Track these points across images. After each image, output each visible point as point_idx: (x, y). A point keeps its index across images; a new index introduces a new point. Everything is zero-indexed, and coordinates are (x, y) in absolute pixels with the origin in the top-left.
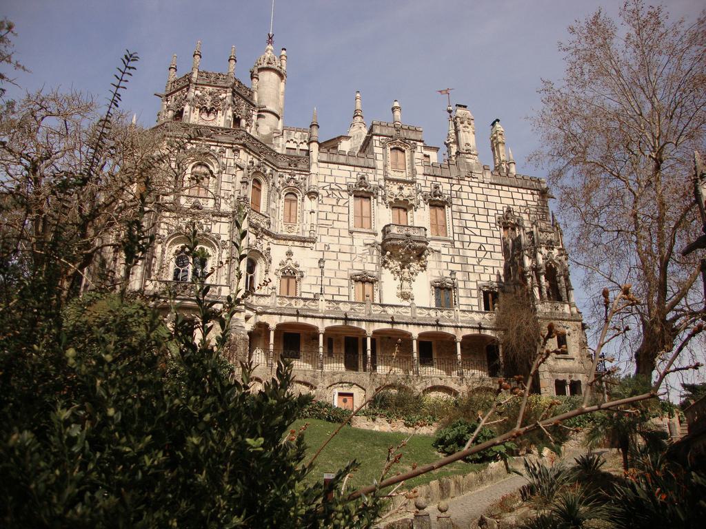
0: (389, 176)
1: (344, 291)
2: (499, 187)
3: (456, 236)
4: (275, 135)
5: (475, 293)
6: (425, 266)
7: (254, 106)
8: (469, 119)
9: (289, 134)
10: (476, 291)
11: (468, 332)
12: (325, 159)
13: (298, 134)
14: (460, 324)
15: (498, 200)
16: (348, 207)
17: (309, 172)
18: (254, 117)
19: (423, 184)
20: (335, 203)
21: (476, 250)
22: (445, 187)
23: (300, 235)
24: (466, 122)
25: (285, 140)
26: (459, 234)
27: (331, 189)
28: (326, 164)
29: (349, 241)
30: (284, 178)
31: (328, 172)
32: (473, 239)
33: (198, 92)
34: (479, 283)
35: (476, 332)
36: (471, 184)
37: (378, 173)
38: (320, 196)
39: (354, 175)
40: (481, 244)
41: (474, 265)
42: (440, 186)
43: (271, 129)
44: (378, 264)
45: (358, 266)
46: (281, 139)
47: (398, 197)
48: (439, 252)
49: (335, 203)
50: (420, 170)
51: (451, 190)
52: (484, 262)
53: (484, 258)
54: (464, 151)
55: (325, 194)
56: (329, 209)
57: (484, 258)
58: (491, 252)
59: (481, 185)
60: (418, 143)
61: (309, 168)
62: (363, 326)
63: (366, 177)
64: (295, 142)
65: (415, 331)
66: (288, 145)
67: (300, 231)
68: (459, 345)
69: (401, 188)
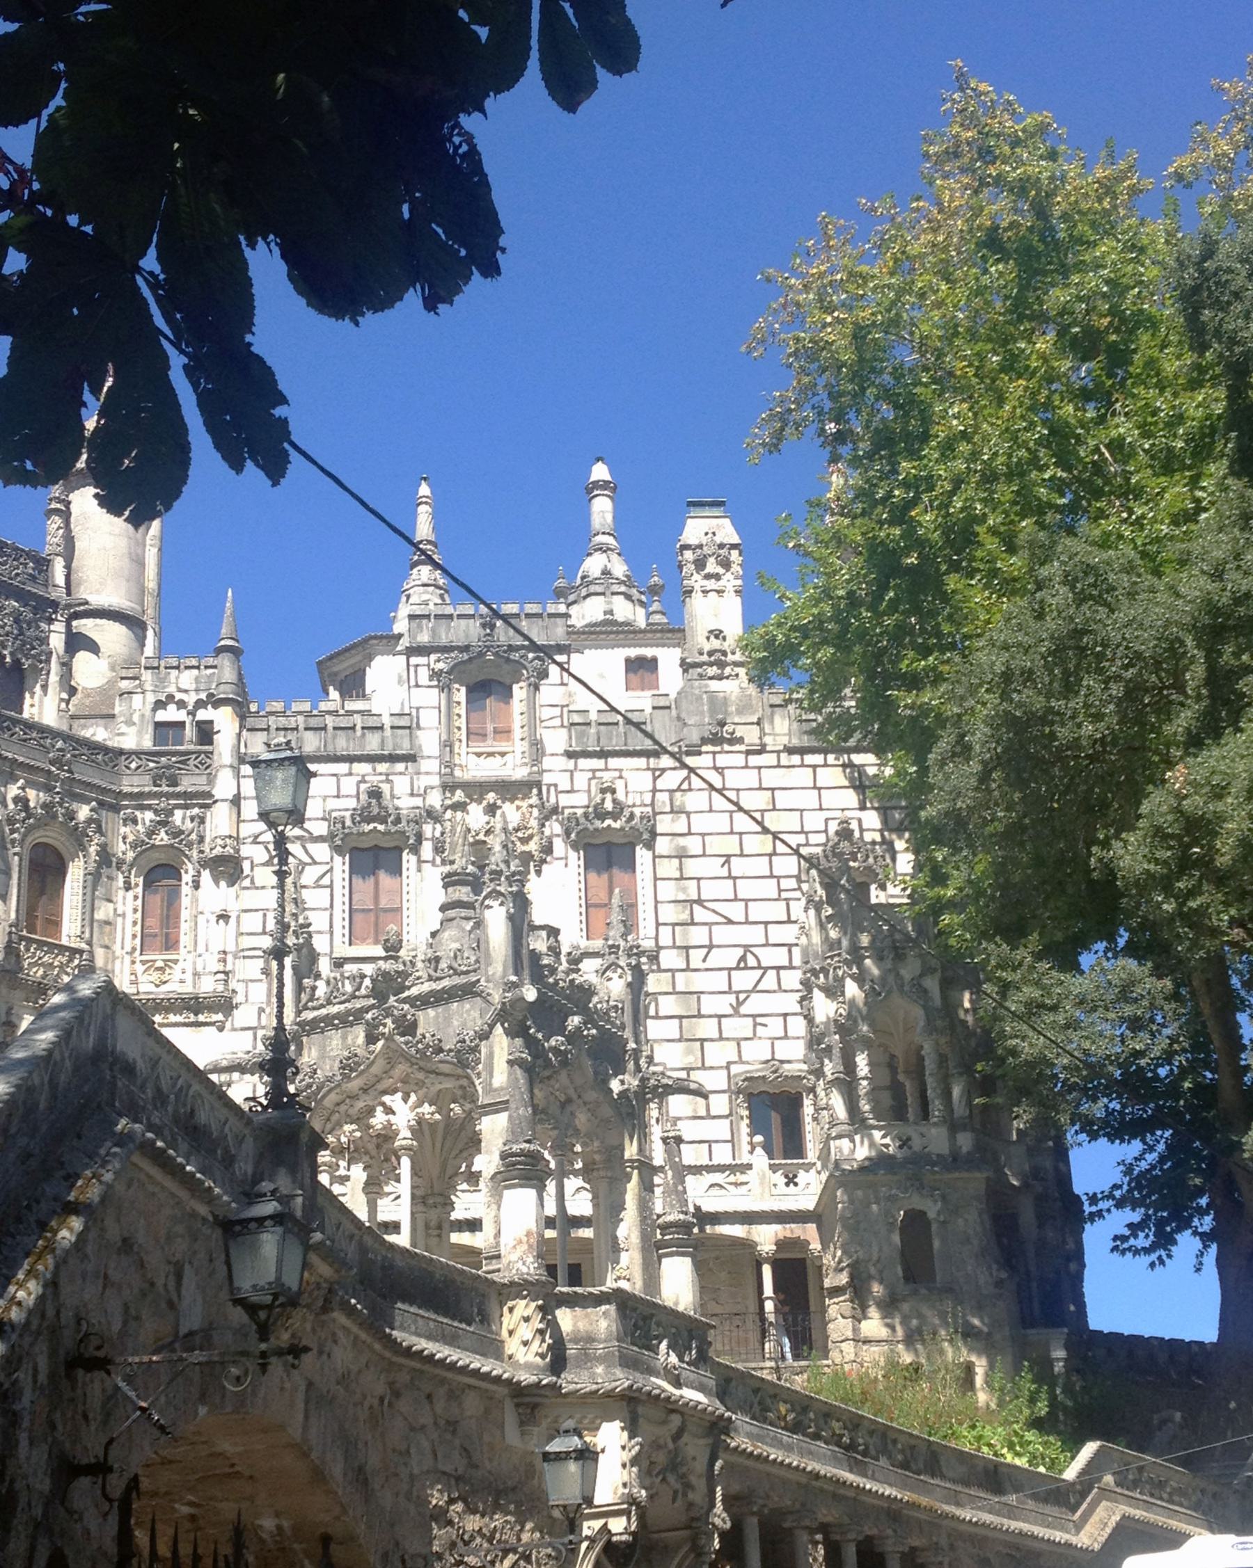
0: (458, 773)
2: (817, 759)
3: (665, 934)
4: (125, 685)
5: (720, 1104)
7: (54, 604)
8: (721, 546)
9: (161, 682)
10: (726, 1096)
15: (810, 799)
16: (331, 886)
17: (209, 795)
19: (564, 785)
21: (730, 969)
22: (634, 781)
23: (190, 990)
24: (712, 560)
25: (151, 698)
26: (674, 925)
30: (140, 827)
32: (722, 934)
34: (735, 1069)
36: (722, 760)
37: (423, 770)
38: (246, 866)
39: (349, 786)
40: (747, 948)
41: (720, 1017)
42: (619, 786)
43: (113, 669)
46: (137, 700)
47: (481, 837)
50: (556, 740)
51: (654, 791)
52: (754, 1004)
53: (754, 990)
54: (705, 658)
57: (754, 990)
58: (778, 968)
59: (754, 760)
61: (211, 780)
63: (385, 788)
64: (181, 704)
66: (162, 716)
67: (188, 977)
69: (491, 810)
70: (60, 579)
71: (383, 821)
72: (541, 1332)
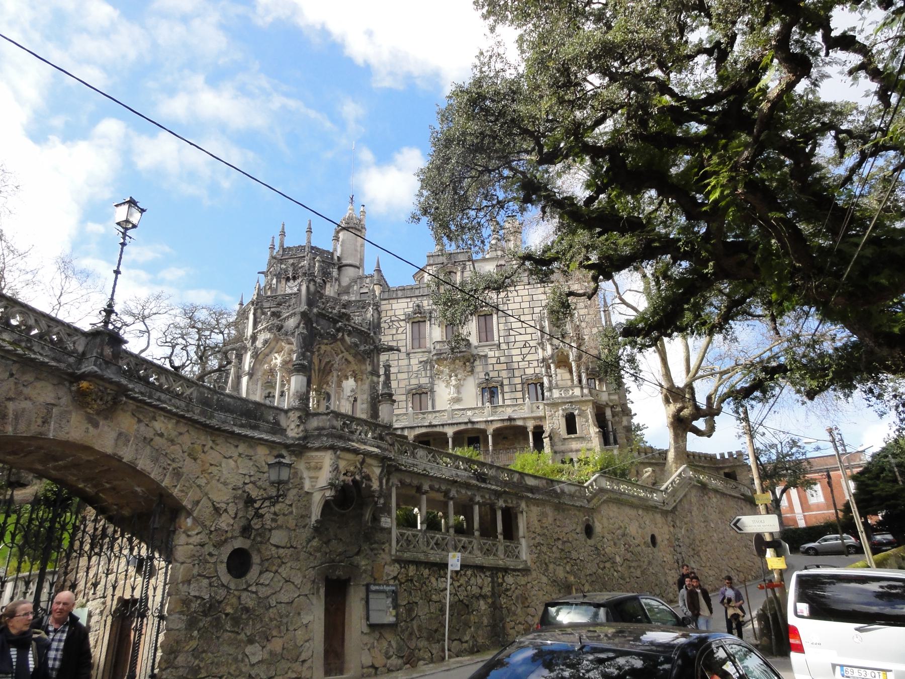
1: (403, 404)
5: (519, 387)
6: (472, 371)
11: (499, 425)
12: (386, 297)
13: (368, 280)
14: (489, 419)
18: (335, 272)
20: (394, 332)
27: (392, 321)
28: (387, 302)
29: (405, 362)
31: (389, 307)
32: (518, 338)
33: (283, 266)
35: (506, 424)
39: (411, 305)
44: (431, 377)
45: (414, 382)
46: (355, 288)
48: (486, 356)
49: (394, 332)
52: (529, 358)
55: (386, 326)
56: (390, 338)
59: (527, 287)
60: (468, 263)
62: (406, 433)
65: (450, 431)
68: (490, 437)
70: (336, 258)
71: (420, 313)
72: (298, 426)
